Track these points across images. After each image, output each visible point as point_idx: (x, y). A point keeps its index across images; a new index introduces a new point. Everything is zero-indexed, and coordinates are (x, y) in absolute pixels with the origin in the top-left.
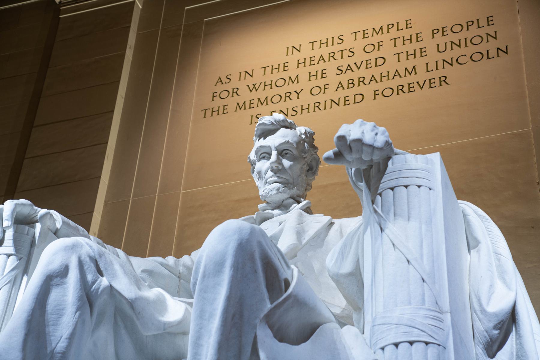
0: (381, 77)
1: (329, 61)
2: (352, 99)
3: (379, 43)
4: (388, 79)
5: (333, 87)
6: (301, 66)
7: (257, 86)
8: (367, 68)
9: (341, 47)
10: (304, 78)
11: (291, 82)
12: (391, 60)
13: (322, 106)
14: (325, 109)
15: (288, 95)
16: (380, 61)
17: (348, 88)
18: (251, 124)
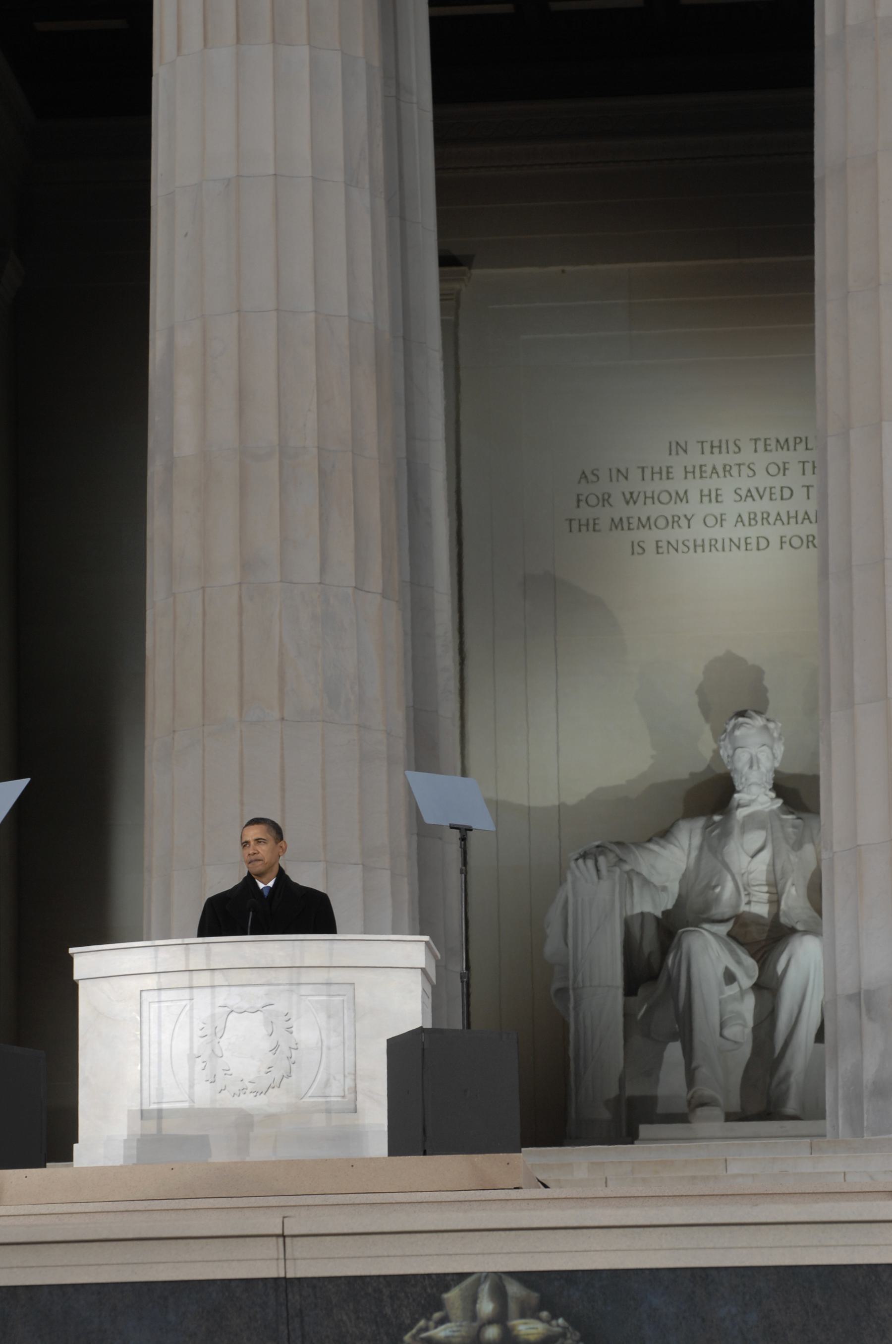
0: (789, 518)
1: (725, 476)
2: (753, 541)
3: (784, 463)
4: (797, 523)
5: (731, 519)
6: (690, 476)
7: (635, 496)
8: (771, 499)
9: (738, 458)
10: (694, 496)
11: (678, 500)
12: (800, 493)
13: (719, 546)
14: (723, 550)
15: (674, 521)
16: (786, 493)
17: (750, 525)
18: (633, 553)
